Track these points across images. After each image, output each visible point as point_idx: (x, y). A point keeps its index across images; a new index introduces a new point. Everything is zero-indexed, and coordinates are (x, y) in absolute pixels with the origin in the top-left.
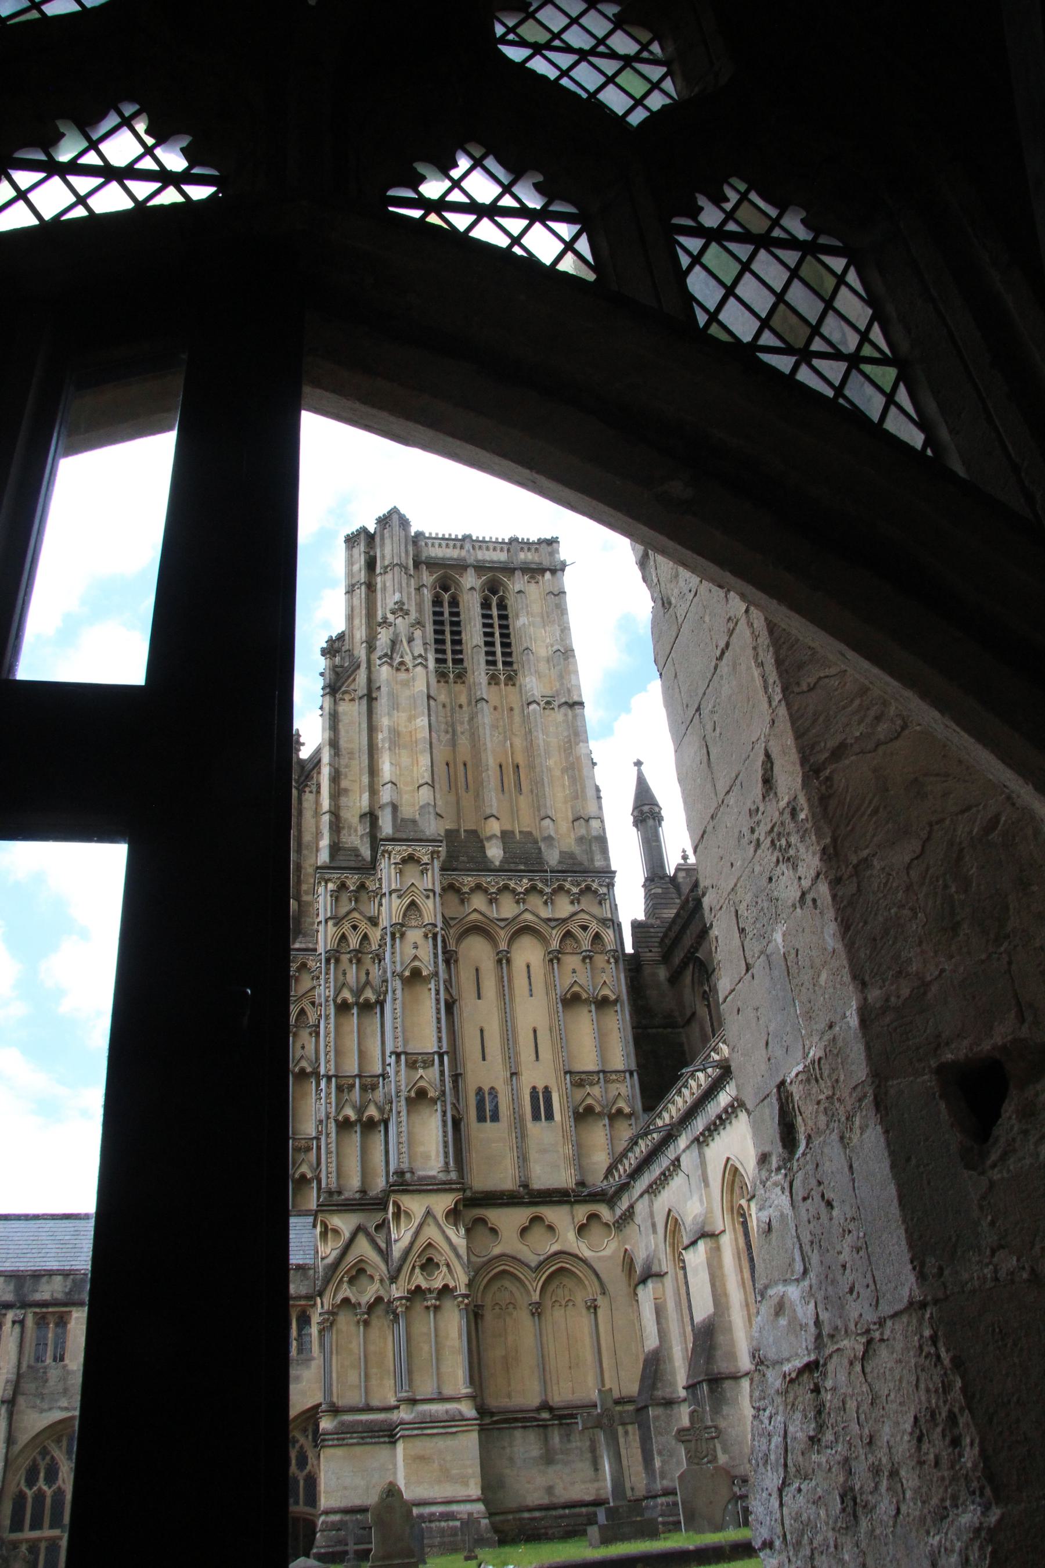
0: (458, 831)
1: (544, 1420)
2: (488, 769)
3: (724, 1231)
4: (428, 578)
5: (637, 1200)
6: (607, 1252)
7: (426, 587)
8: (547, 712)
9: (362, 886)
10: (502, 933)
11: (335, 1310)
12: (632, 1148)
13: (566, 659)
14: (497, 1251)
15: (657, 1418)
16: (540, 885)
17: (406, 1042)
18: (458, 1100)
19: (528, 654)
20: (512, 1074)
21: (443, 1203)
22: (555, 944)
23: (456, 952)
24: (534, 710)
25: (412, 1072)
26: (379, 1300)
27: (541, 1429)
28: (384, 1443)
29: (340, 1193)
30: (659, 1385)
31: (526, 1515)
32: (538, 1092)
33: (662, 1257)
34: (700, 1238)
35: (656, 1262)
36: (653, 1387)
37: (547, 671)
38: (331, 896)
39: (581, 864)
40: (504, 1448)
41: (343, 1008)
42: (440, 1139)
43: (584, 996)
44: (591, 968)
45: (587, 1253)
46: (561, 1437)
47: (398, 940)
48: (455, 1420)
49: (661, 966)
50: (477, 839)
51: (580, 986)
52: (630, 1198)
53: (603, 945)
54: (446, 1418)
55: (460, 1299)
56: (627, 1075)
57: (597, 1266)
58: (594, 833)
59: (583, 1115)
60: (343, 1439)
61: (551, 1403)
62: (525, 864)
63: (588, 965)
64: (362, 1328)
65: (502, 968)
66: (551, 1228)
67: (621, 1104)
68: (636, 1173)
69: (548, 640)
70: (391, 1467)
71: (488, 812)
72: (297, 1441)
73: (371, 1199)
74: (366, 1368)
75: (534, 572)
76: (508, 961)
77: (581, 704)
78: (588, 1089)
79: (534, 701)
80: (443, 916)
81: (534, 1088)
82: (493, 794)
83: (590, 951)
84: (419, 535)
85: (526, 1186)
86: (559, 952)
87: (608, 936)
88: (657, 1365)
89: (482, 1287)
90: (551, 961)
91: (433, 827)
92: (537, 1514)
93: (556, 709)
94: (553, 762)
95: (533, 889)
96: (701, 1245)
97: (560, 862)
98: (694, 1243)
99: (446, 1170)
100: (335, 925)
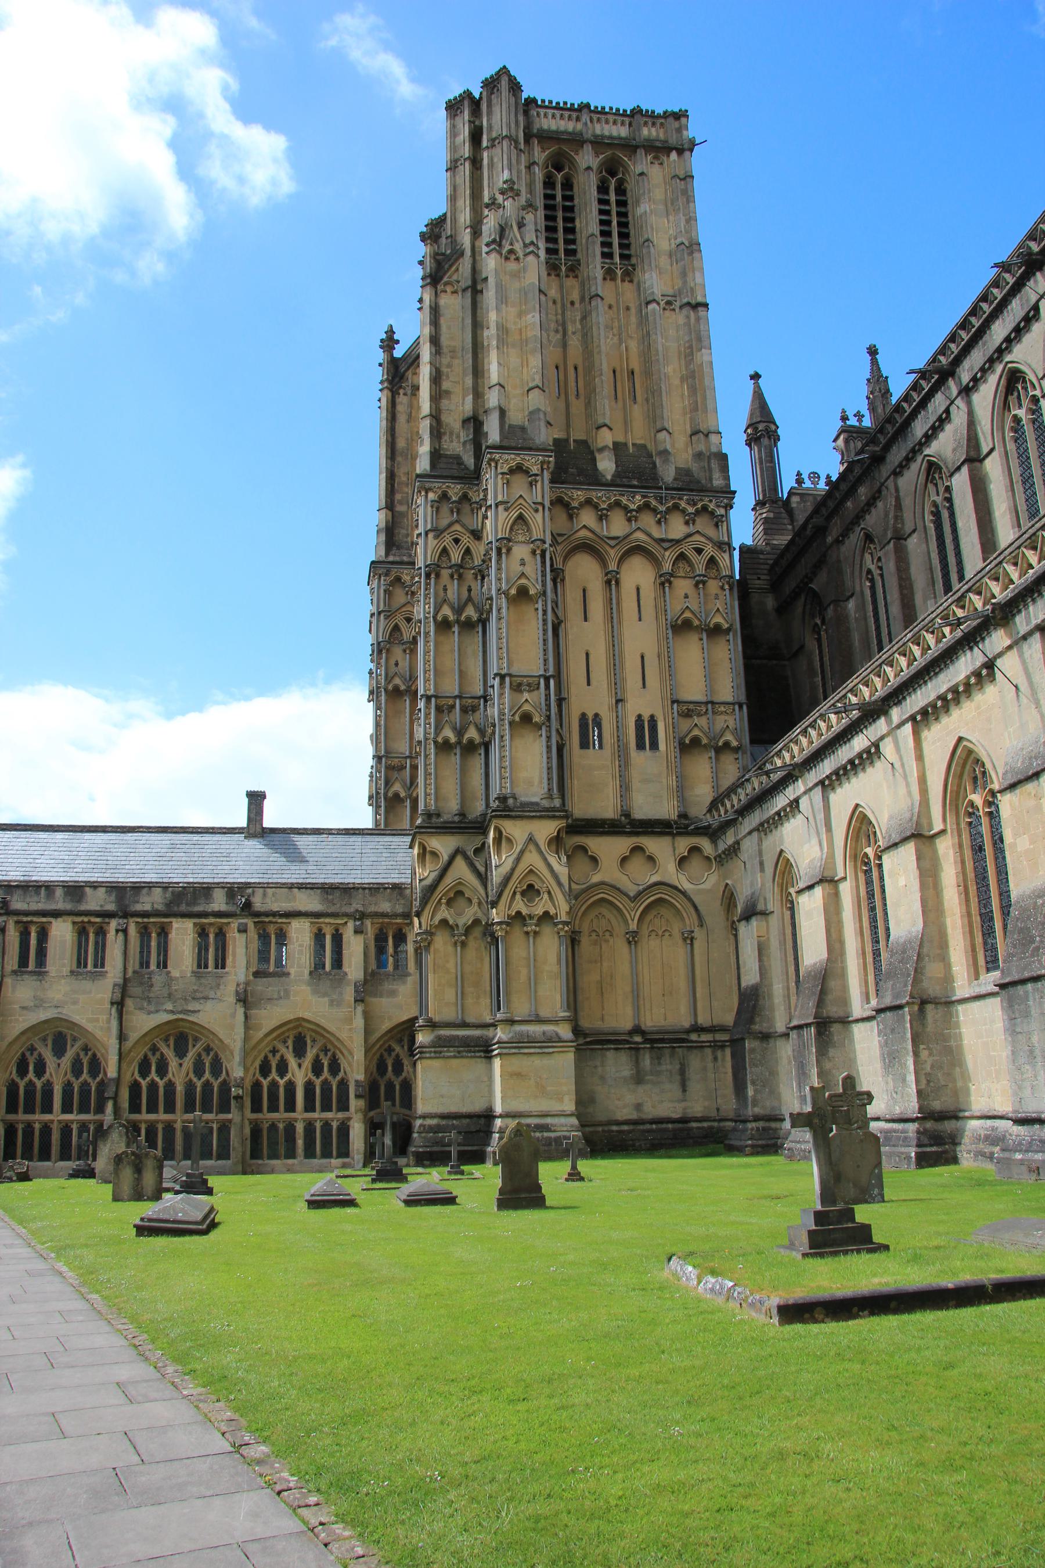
0: (567, 440)
1: (636, 1043)
2: (601, 374)
3: (844, 878)
4: (540, 155)
5: (745, 837)
6: (707, 886)
7: (538, 164)
8: (667, 313)
9: (465, 497)
10: (612, 552)
11: (433, 930)
12: (742, 784)
13: (691, 253)
14: (596, 879)
15: (752, 1051)
16: (654, 503)
17: (510, 664)
18: (561, 725)
19: (648, 246)
20: (618, 701)
21: (546, 829)
22: (667, 567)
23: (563, 571)
24: (654, 310)
25: (517, 695)
26: (476, 922)
27: (633, 1052)
28: (480, 1057)
29: (438, 815)
30: (757, 1019)
31: (615, 1128)
32: (643, 721)
33: (769, 896)
34: (817, 883)
35: (762, 901)
36: (751, 1021)
37: (669, 267)
38: (432, 507)
39: (699, 482)
40: (596, 1067)
41: (444, 626)
42: (545, 765)
43: (696, 623)
44: (705, 595)
45: (686, 886)
46: (651, 1058)
47: (504, 556)
48: (551, 1041)
49: (770, 595)
50: (587, 451)
51: (692, 612)
52: (736, 834)
53: (718, 570)
54: (543, 1039)
55: (560, 926)
56: (737, 707)
57: (697, 899)
58: (714, 449)
59: (688, 746)
60: (441, 1052)
61: (643, 1027)
62: (639, 479)
63: (701, 591)
64: (459, 948)
65: (611, 590)
66: (651, 859)
67: (729, 737)
68: (745, 810)
69: (671, 232)
70: (486, 1079)
71: (600, 421)
72: (394, 1050)
73: (470, 822)
74: (463, 987)
75: (659, 150)
76: (617, 583)
77: (706, 305)
78: (696, 720)
79: (654, 301)
80: (552, 534)
81: (639, 716)
82: (606, 401)
83: (704, 576)
84: (531, 102)
85: (627, 815)
86: (672, 575)
87: (723, 560)
88: (757, 1000)
89: (580, 914)
90: (662, 584)
91: (544, 436)
92: (625, 1128)
93: (677, 310)
94: (672, 369)
95: (647, 506)
96: (818, 891)
97: (675, 479)
98: (810, 887)
99: (550, 797)
100: (436, 537)
